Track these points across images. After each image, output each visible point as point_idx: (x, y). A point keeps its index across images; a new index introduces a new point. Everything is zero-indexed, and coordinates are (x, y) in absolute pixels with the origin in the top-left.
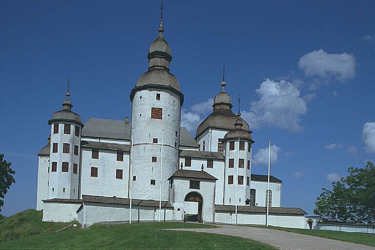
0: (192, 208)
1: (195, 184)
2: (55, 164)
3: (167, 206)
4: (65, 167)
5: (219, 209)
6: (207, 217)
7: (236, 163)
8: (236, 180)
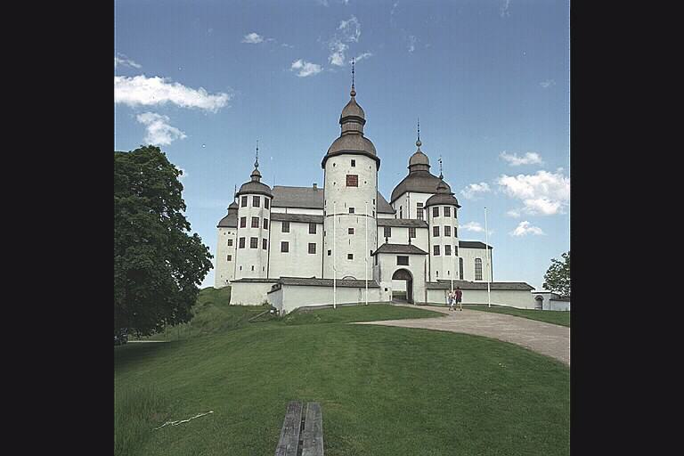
0: (401, 286)
1: (403, 260)
2: (242, 240)
3: (373, 285)
4: (254, 243)
5: (430, 287)
6: (419, 296)
7: (442, 231)
8: (443, 250)
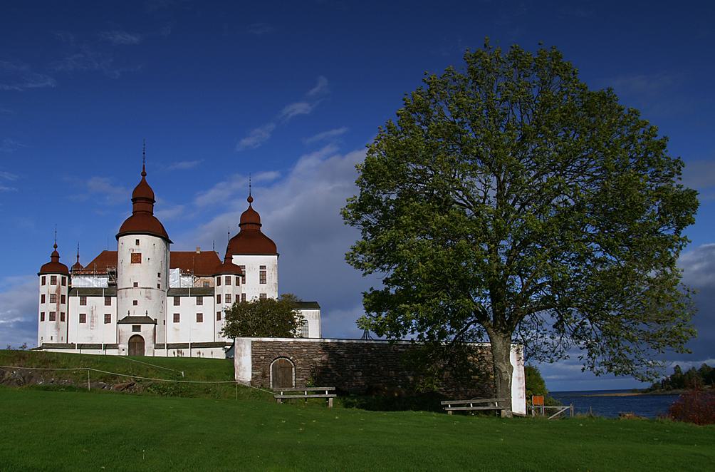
3: (115, 346)
